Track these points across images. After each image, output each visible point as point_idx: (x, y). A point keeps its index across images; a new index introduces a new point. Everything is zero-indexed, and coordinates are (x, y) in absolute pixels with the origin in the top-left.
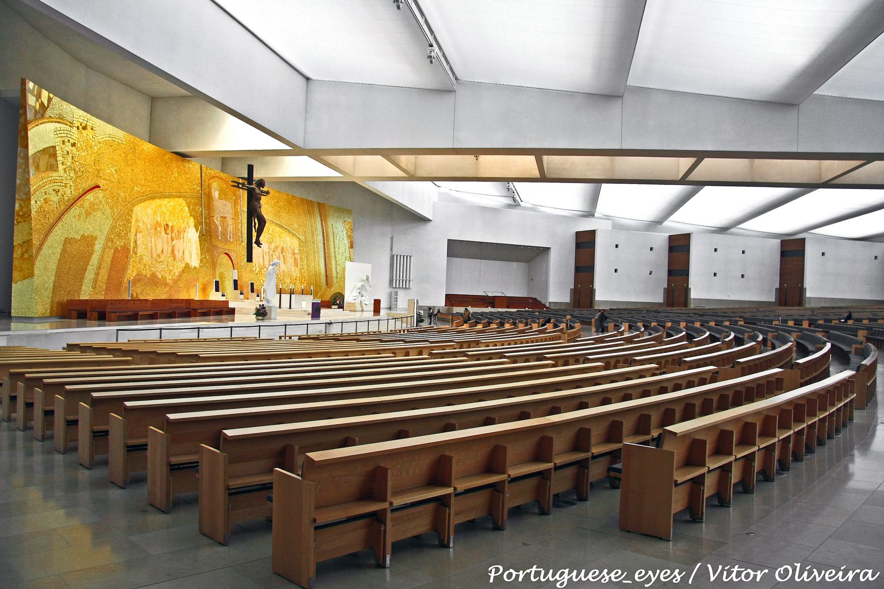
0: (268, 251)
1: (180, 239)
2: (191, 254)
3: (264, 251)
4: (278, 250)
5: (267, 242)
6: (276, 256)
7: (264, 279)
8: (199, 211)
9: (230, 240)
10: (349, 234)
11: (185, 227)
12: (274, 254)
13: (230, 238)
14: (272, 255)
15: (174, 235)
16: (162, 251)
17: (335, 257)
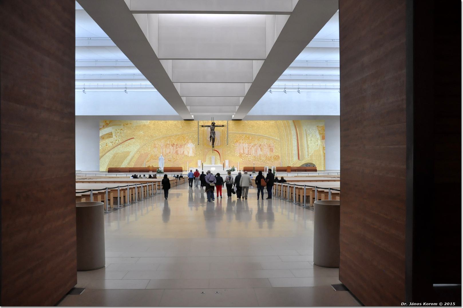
0: (248, 147)
1: (182, 147)
2: (189, 152)
3: (245, 147)
4: (256, 146)
5: (247, 143)
6: (254, 149)
7: (243, 158)
8: (196, 137)
9: (218, 145)
10: (321, 132)
11: (186, 143)
12: (252, 147)
13: (218, 144)
14: (251, 148)
15: (177, 147)
16: (170, 152)
17: (308, 145)
